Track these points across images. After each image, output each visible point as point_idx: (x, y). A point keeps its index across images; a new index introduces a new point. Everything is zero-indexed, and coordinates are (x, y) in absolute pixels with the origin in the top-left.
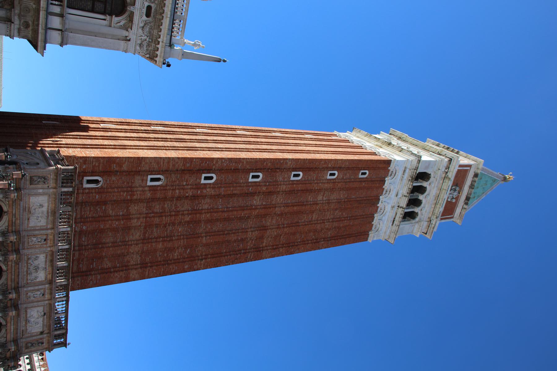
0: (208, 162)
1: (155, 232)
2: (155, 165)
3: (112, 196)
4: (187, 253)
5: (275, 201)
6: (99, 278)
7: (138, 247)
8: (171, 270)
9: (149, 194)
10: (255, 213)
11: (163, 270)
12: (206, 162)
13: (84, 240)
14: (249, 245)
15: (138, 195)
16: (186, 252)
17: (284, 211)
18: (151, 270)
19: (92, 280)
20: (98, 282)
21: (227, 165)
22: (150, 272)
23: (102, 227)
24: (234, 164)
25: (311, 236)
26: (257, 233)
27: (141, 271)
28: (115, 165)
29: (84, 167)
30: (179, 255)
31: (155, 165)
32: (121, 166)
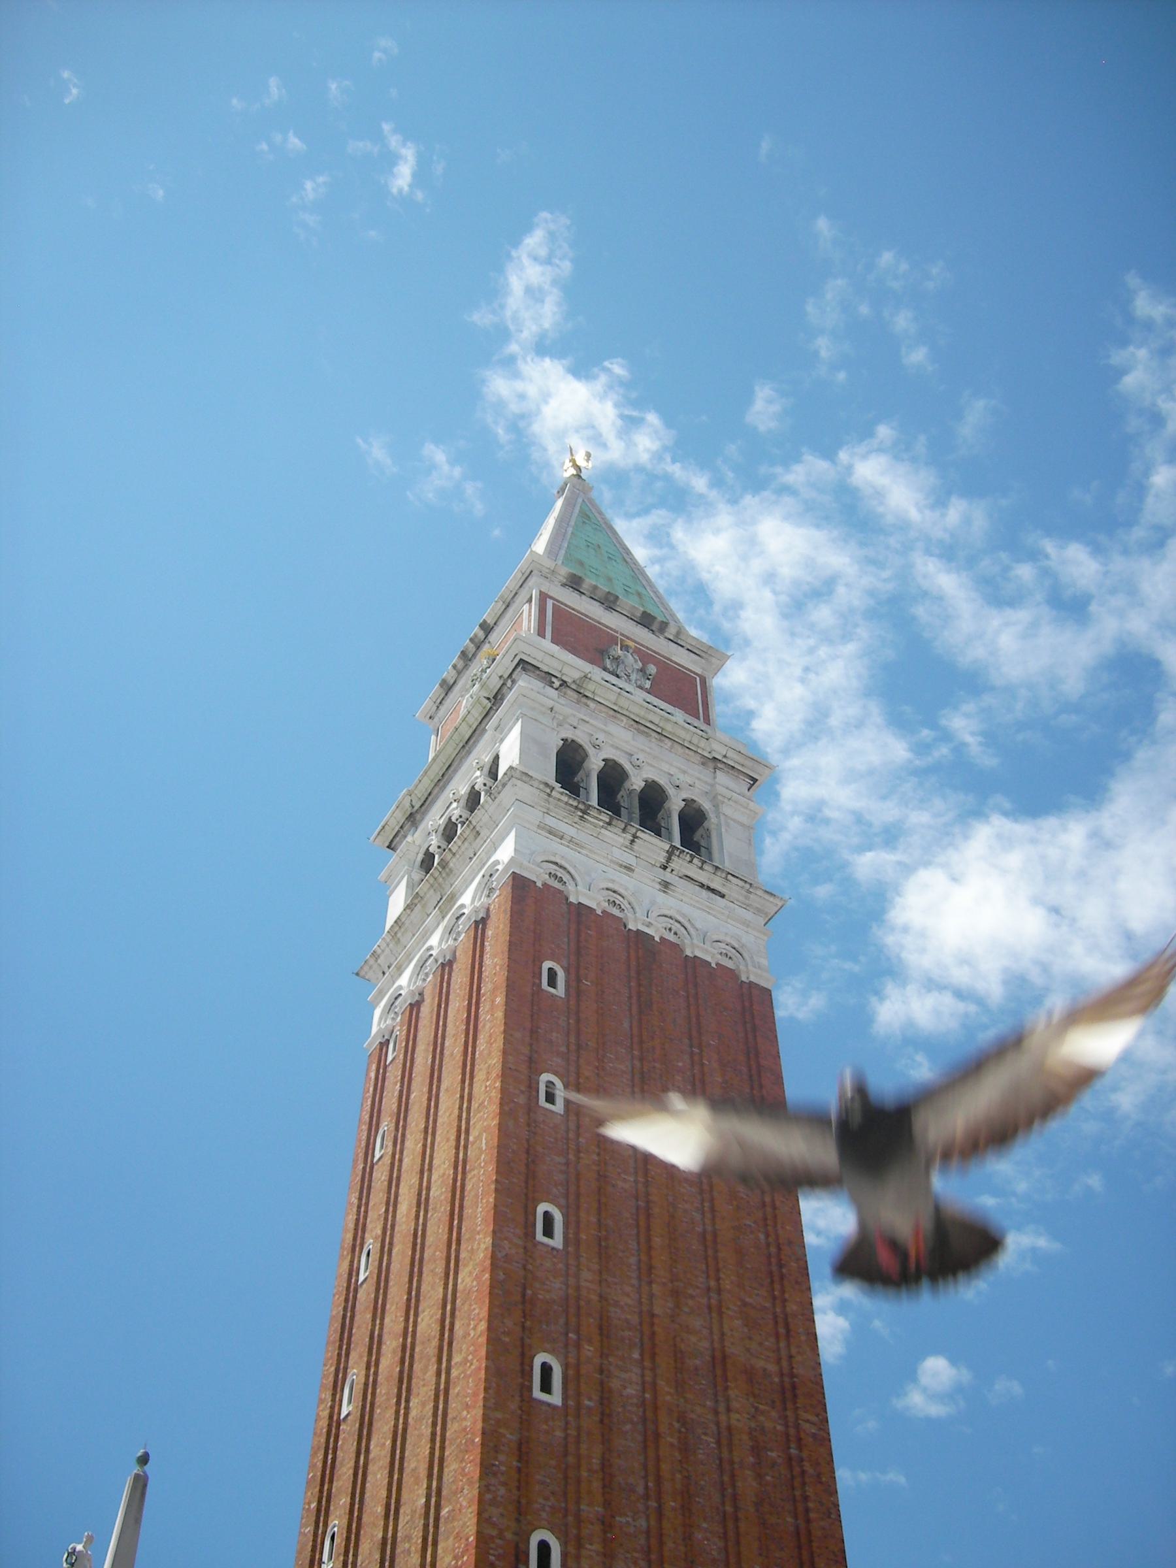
10: (669, 1393)
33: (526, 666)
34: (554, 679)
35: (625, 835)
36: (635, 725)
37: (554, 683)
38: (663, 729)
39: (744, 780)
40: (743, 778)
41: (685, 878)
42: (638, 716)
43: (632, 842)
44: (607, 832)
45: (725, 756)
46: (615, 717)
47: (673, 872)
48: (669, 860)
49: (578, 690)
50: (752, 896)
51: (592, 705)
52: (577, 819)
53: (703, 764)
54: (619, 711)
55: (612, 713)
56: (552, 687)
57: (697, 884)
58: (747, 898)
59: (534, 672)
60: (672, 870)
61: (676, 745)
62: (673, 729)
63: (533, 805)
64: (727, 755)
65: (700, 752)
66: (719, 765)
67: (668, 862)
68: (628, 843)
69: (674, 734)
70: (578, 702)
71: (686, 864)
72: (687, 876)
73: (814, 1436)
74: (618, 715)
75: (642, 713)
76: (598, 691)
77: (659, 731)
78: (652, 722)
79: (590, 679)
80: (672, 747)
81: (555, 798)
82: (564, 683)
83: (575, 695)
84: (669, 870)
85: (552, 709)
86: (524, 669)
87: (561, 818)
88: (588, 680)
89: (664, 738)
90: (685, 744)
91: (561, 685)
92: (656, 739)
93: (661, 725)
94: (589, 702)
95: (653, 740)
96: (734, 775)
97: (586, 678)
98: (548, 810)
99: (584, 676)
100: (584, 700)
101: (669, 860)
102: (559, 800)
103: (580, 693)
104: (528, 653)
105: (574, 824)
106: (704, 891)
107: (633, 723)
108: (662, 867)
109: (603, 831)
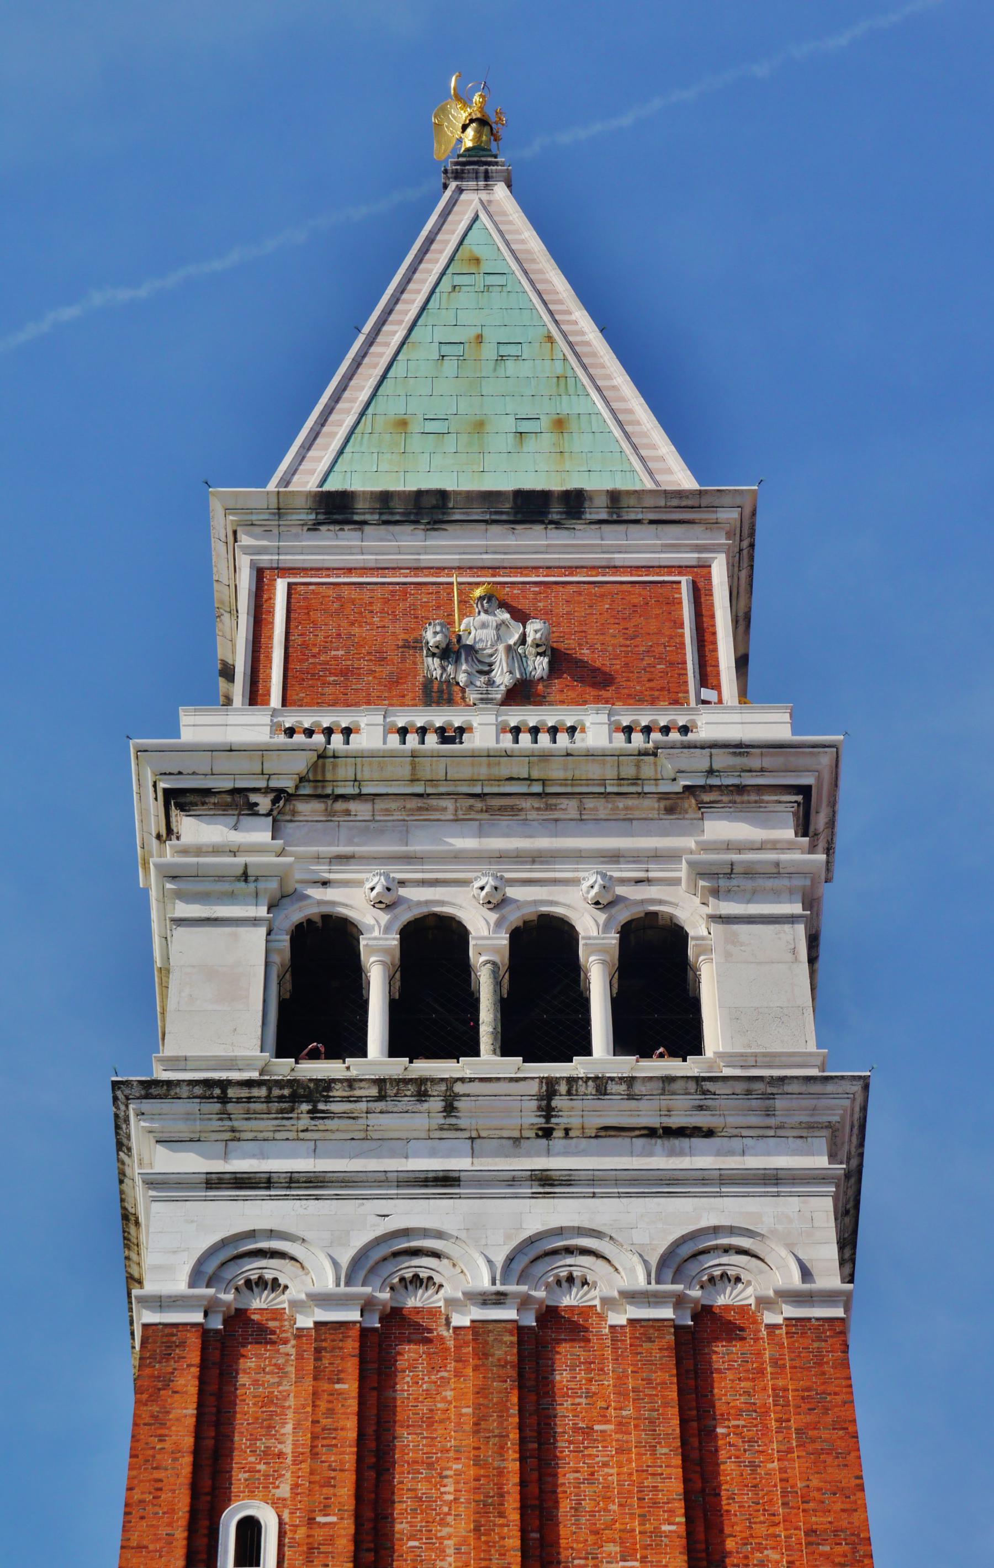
33: (182, 800)
34: (254, 798)
35: (426, 1105)
36: (479, 804)
37: (256, 804)
38: (544, 782)
39: (780, 802)
40: (775, 798)
41: (603, 1133)
42: (473, 781)
43: (449, 1109)
44: (385, 1120)
45: (711, 772)
46: (427, 809)
47: (571, 1134)
48: (548, 1111)
49: (319, 792)
50: (779, 1103)
51: (361, 809)
52: (305, 1122)
53: (670, 810)
54: (429, 790)
55: (413, 804)
56: (256, 814)
57: (637, 1133)
58: (769, 1112)
59: (204, 804)
60: (567, 1131)
61: (589, 803)
62: (566, 769)
63: (196, 1136)
64: (715, 767)
65: (653, 789)
66: (706, 798)
67: (548, 1118)
68: (439, 1120)
69: (574, 781)
70: (330, 813)
71: (590, 1104)
72: (606, 1128)
74: (434, 802)
75: (483, 772)
76: (365, 774)
77: (537, 788)
78: (511, 779)
79: (334, 757)
80: (581, 809)
81: (239, 1100)
82: (279, 795)
83: (318, 806)
84: (558, 1133)
85: (245, 876)
86: (182, 807)
87: (270, 1135)
88: (332, 760)
89: (552, 801)
90: (609, 789)
91: (275, 802)
92: (538, 809)
93: (535, 775)
94: (353, 806)
95: (533, 815)
96: (749, 802)
97: (325, 757)
98: (233, 1131)
99: (319, 757)
100: (340, 806)
101: (548, 1111)
102: (249, 1100)
103: (327, 796)
104: (176, 771)
105: (302, 1135)
106: (659, 1141)
107: (471, 801)
108: (540, 1133)
109: (374, 1120)
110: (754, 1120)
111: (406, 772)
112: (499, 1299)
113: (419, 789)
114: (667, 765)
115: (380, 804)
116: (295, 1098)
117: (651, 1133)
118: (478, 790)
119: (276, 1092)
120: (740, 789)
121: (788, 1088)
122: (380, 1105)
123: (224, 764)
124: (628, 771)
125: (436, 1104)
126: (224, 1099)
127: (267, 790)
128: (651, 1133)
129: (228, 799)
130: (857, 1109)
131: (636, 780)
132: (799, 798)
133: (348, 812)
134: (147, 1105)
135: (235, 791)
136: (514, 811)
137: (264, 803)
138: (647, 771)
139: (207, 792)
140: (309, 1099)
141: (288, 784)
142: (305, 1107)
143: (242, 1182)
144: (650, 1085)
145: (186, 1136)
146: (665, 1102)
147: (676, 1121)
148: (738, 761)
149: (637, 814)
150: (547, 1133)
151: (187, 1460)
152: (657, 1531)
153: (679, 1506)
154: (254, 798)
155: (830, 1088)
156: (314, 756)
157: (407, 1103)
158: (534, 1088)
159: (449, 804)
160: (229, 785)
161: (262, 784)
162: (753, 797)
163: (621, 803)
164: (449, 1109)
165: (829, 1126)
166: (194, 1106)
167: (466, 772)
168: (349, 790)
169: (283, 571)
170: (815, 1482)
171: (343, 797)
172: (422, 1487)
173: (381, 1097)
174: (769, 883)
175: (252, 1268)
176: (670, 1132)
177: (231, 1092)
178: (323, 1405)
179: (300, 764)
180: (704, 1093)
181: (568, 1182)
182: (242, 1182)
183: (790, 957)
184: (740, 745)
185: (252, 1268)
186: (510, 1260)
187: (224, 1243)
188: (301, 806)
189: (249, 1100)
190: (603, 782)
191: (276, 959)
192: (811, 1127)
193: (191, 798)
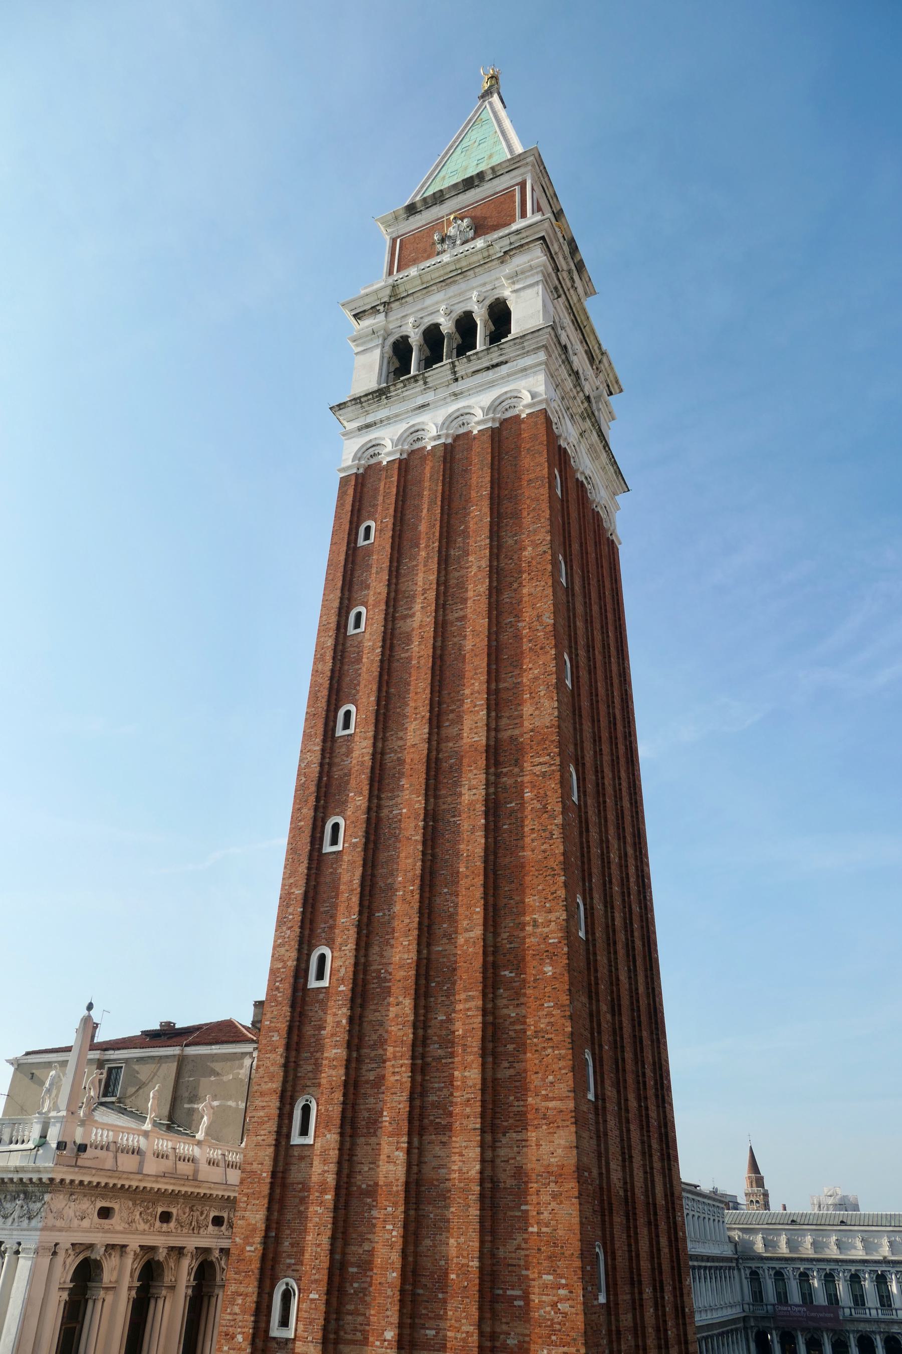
0: (277, 984)
1: (439, 1096)
2: (262, 1132)
3: (319, 1250)
4: (513, 975)
5: (400, 752)
6: (551, 1277)
7: (466, 1147)
8: (552, 1020)
9: (328, 1136)
11: (549, 1051)
12: (277, 989)
13: (433, 1332)
14: (513, 780)
15: (326, 1168)
16: (512, 980)
17: (423, 717)
18: (543, 1092)
19: (554, 1305)
20: (563, 1281)
21: (289, 928)
22: (550, 1095)
23: (395, 1274)
24: (290, 910)
25: (513, 595)
26: (475, 772)
27: (545, 1127)
28: (248, 1248)
29: (240, 1338)
30: (516, 1002)
31: (262, 1132)
32: (254, 1230)
34: (378, 308)
36: (443, 284)
38: (461, 268)
43: (425, 383)
48: (455, 373)
52: (385, 401)
53: (502, 263)
58: (523, 348)
61: (477, 270)
70: (402, 304)
72: (474, 372)
73: (544, 774)
74: (430, 289)
75: (442, 272)
76: (408, 287)
77: (459, 271)
80: (475, 273)
83: (397, 303)
89: (465, 274)
91: (384, 307)
93: (458, 267)
94: (407, 299)
95: (461, 281)
100: (404, 301)
110: (518, 353)
111: (419, 282)
112: (439, 436)
113: (425, 286)
114: (497, 247)
115: (415, 295)
116: (380, 395)
117: (488, 368)
118: (442, 279)
119: (375, 395)
120: (522, 246)
121: (527, 338)
122: (405, 389)
123: (367, 300)
124: (486, 254)
125: (421, 382)
126: (361, 403)
127: (381, 304)
128: (488, 368)
129: (371, 311)
130: (554, 337)
131: (489, 256)
132: (541, 241)
133: (406, 302)
134: (341, 412)
135: (373, 308)
136: (455, 282)
137: (381, 308)
138: (491, 252)
139: (364, 311)
140: (384, 394)
141: (386, 299)
142: (384, 397)
143: (368, 426)
144: (483, 353)
145: (354, 417)
146: (490, 356)
147: (495, 362)
148: (519, 236)
149: (492, 268)
150: (456, 380)
151: (350, 513)
152: (482, 495)
153: (489, 485)
154: (378, 308)
155: (541, 333)
156: (391, 287)
157: (413, 385)
158: (448, 366)
159: (434, 287)
160: (370, 307)
161: (379, 303)
162: (527, 247)
163: (486, 266)
164: (425, 383)
165: (543, 346)
166: (354, 407)
167: (437, 275)
168: (405, 294)
169: (399, 237)
170: (532, 464)
171: (403, 298)
172: (416, 502)
173: (405, 386)
174: (529, 273)
175: (371, 451)
176: (494, 366)
177: (362, 400)
178: (387, 486)
179: (388, 291)
180: (501, 349)
181: (462, 393)
182: (368, 426)
183: (536, 295)
184: (517, 231)
185: (371, 451)
186: (443, 424)
187: (363, 446)
188: (395, 305)
189: (368, 400)
190: (479, 261)
191: (386, 355)
192: (538, 348)
193: (361, 315)
